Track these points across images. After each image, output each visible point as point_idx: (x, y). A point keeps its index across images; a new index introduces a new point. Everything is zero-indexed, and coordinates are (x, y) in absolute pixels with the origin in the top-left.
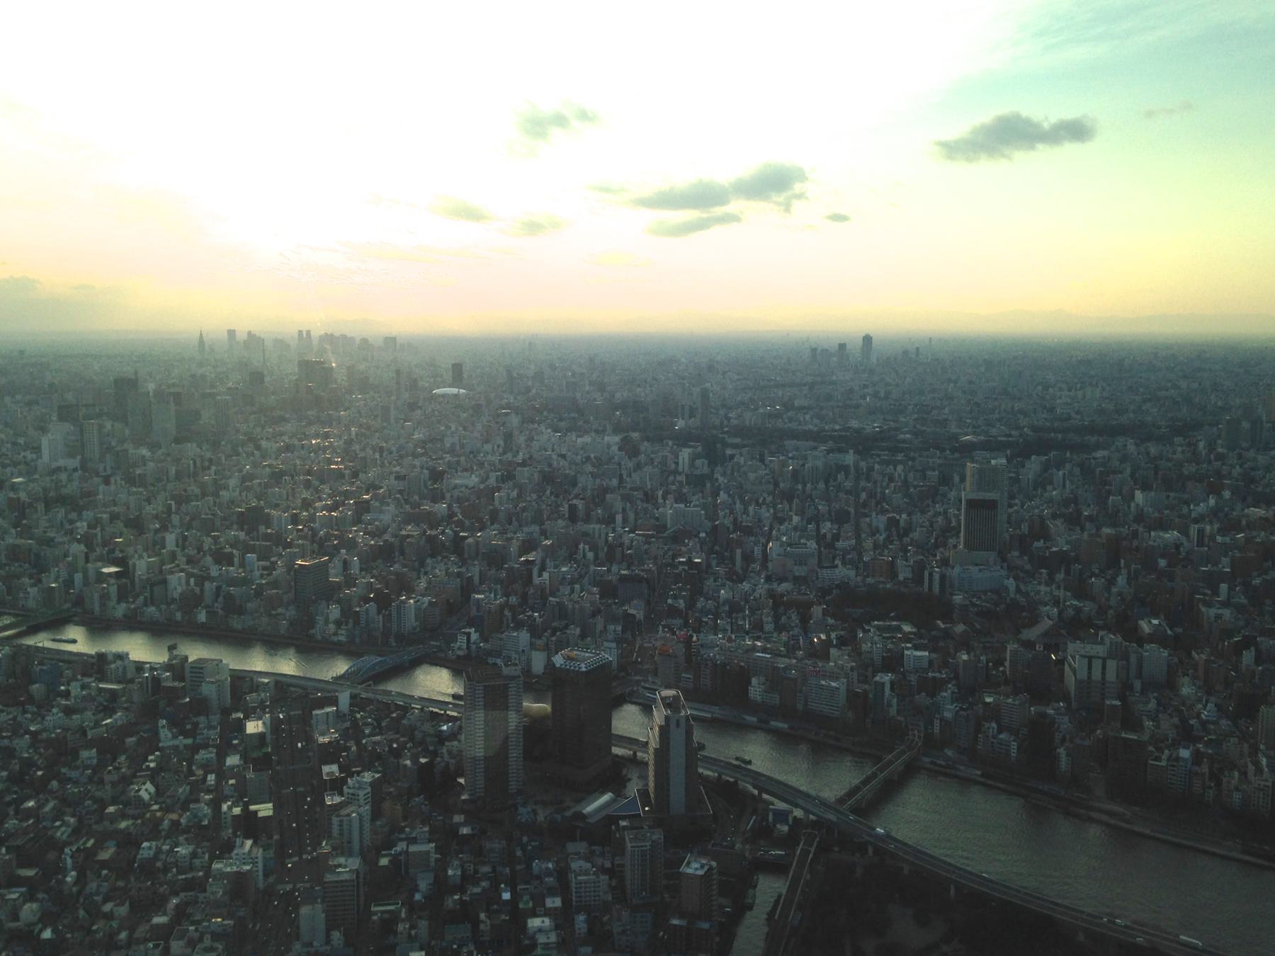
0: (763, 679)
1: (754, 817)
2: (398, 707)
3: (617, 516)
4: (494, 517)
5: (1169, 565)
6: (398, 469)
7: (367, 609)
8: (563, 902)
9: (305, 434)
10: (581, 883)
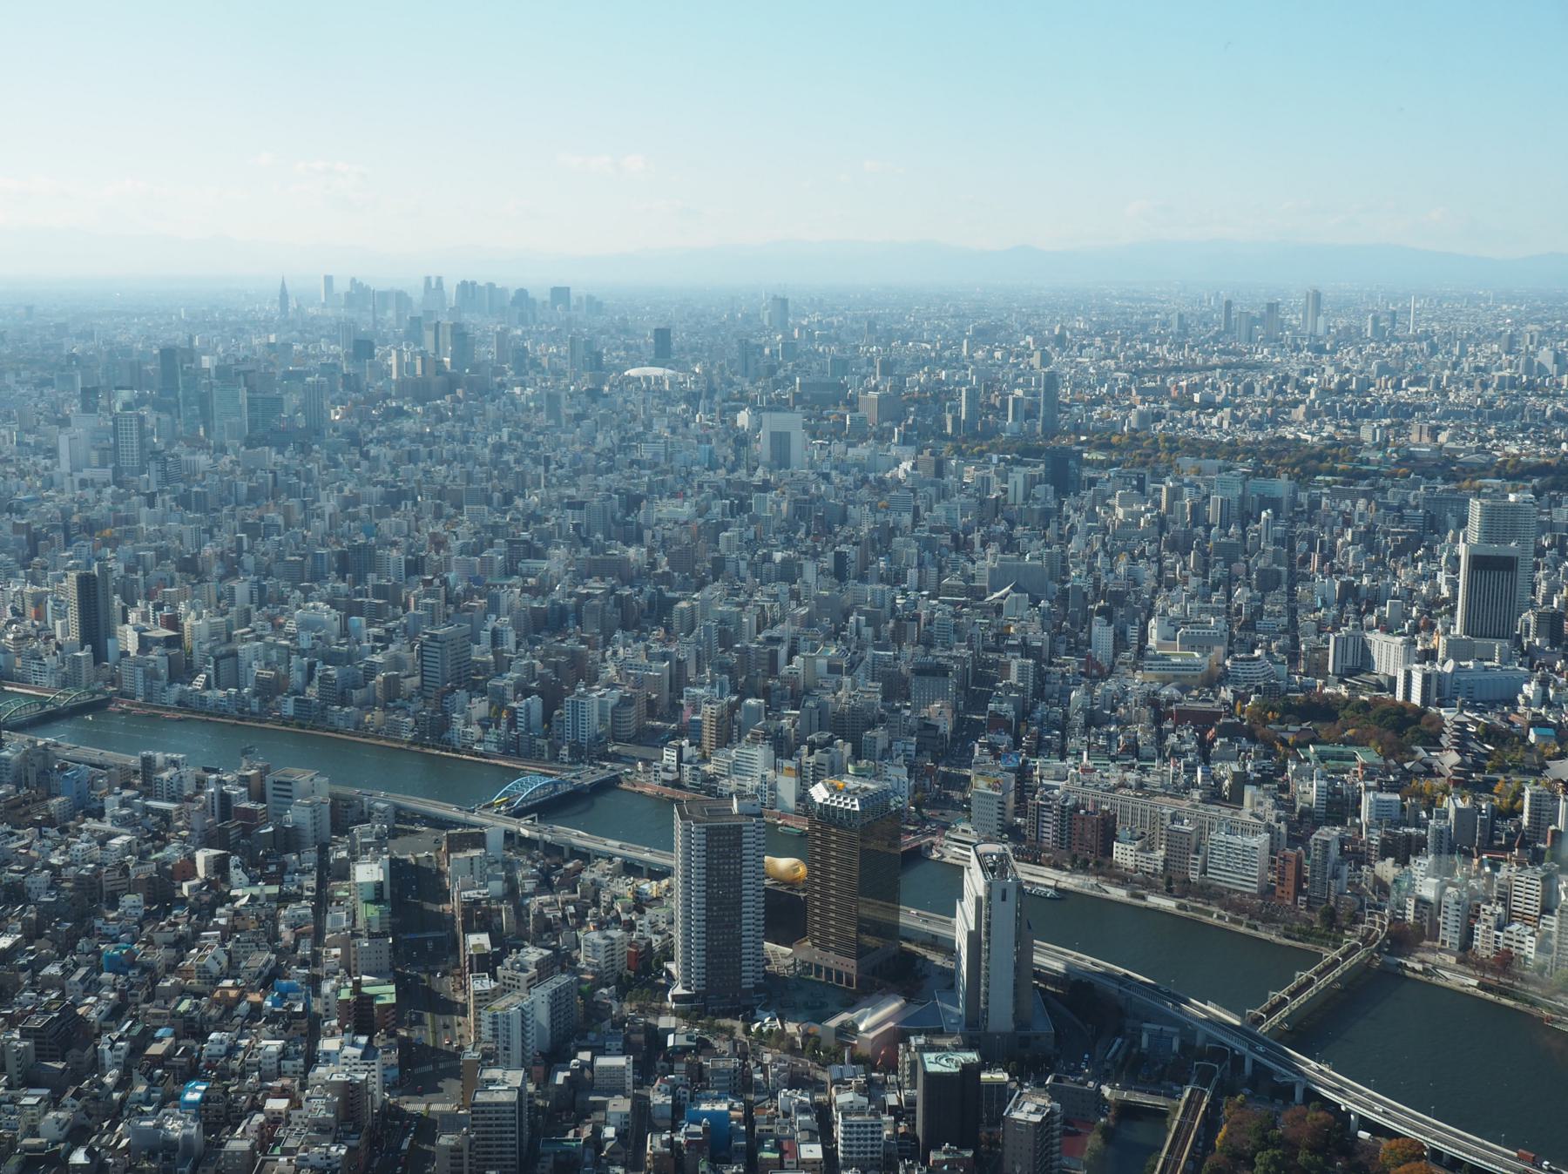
1: (1119, 1040)
2: (576, 853)
3: (909, 572)
4: (718, 568)
6: (572, 491)
7: (527, 705)
8: (824, 1151)
9: (434, 437)
10: (851, 1126)
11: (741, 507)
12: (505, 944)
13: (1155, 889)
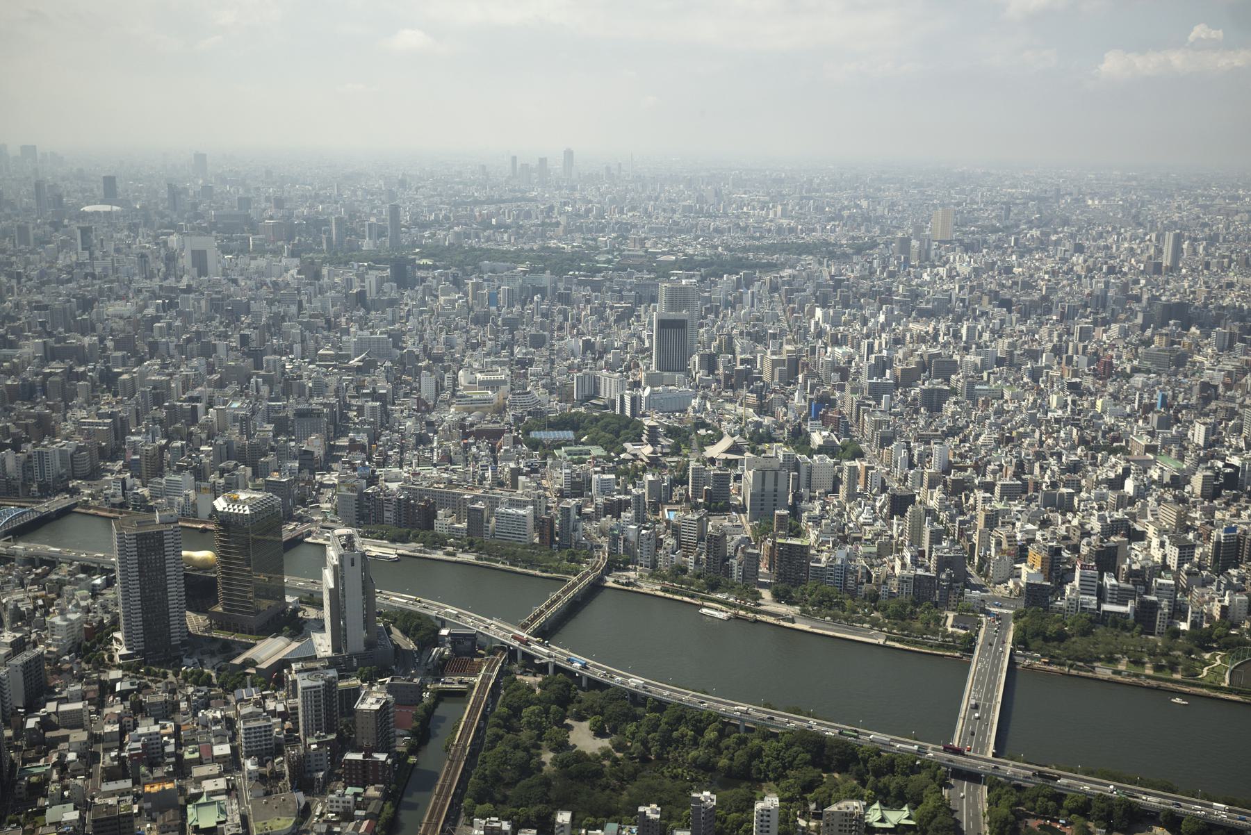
2: (43, 562)
3: (295, 345)
4: (154, 350)
6: (38, 297)
8: (232, 748)
10: (250, 729)
13: (465, 552)
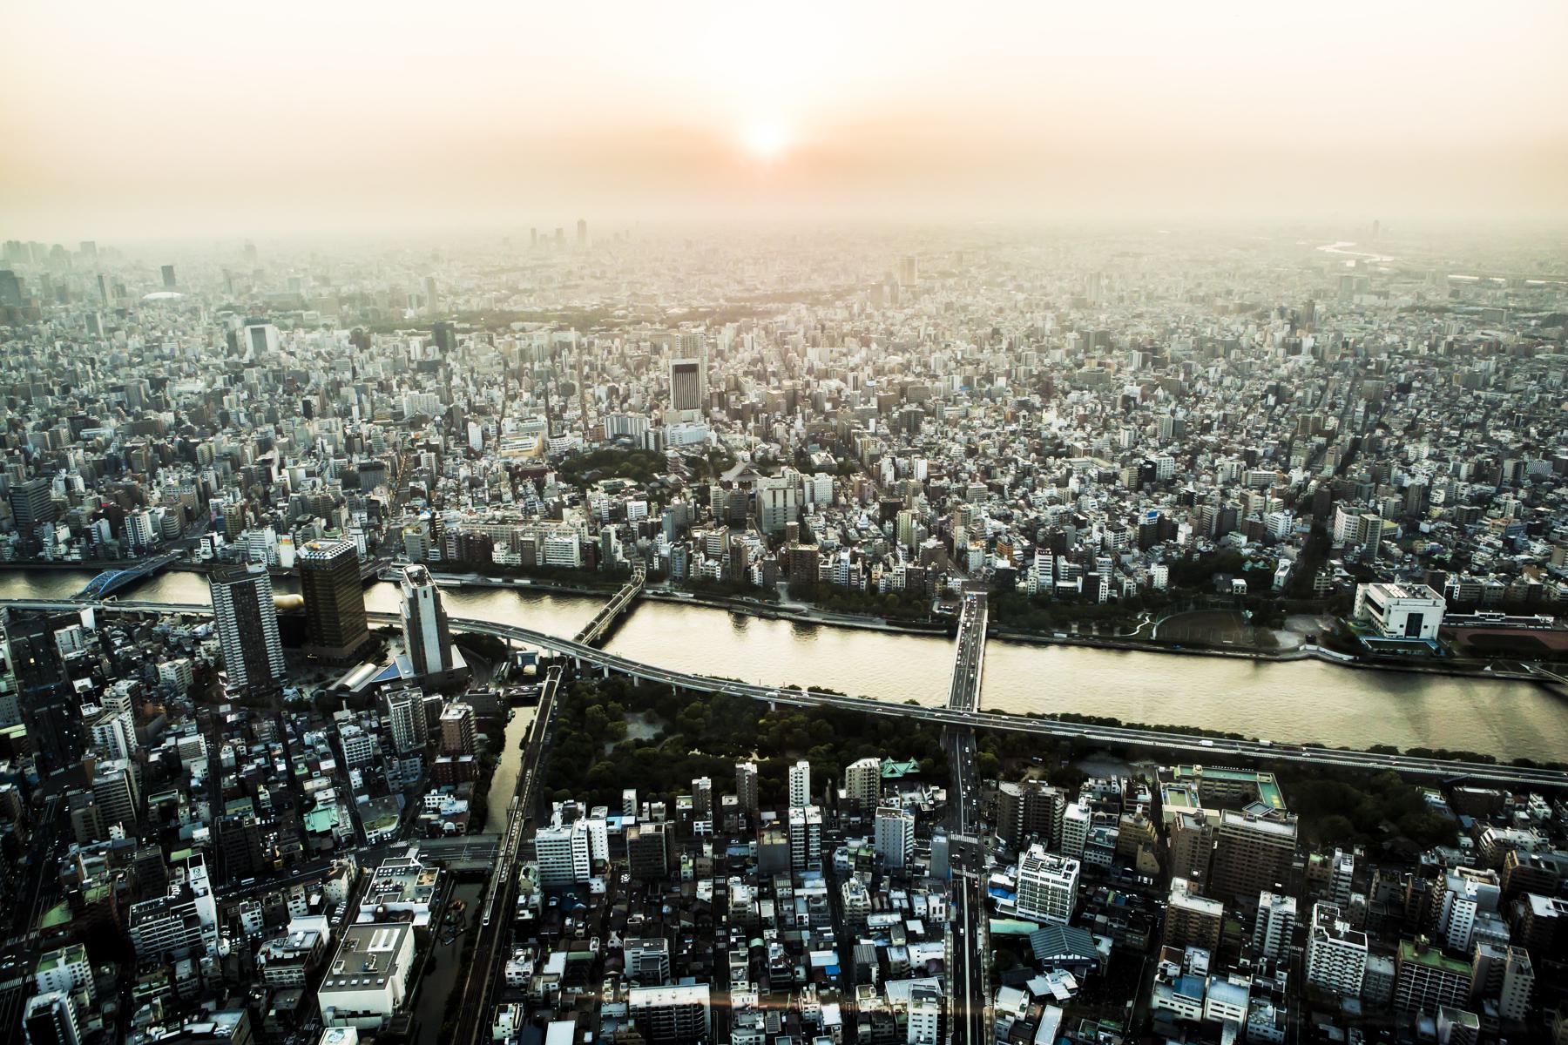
0: (504, 544)
2: (147, 616)
5: (834, 407)
6: (114, 380)
11: (238, 378)
12: (101, 683)
13: (519, 578)
